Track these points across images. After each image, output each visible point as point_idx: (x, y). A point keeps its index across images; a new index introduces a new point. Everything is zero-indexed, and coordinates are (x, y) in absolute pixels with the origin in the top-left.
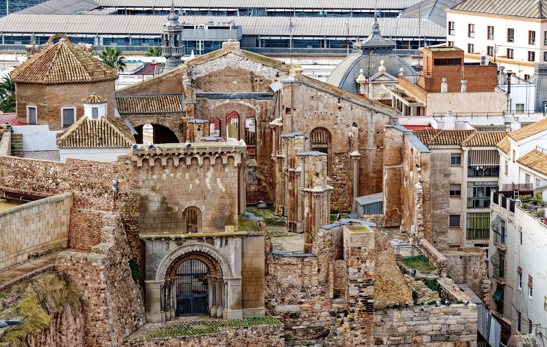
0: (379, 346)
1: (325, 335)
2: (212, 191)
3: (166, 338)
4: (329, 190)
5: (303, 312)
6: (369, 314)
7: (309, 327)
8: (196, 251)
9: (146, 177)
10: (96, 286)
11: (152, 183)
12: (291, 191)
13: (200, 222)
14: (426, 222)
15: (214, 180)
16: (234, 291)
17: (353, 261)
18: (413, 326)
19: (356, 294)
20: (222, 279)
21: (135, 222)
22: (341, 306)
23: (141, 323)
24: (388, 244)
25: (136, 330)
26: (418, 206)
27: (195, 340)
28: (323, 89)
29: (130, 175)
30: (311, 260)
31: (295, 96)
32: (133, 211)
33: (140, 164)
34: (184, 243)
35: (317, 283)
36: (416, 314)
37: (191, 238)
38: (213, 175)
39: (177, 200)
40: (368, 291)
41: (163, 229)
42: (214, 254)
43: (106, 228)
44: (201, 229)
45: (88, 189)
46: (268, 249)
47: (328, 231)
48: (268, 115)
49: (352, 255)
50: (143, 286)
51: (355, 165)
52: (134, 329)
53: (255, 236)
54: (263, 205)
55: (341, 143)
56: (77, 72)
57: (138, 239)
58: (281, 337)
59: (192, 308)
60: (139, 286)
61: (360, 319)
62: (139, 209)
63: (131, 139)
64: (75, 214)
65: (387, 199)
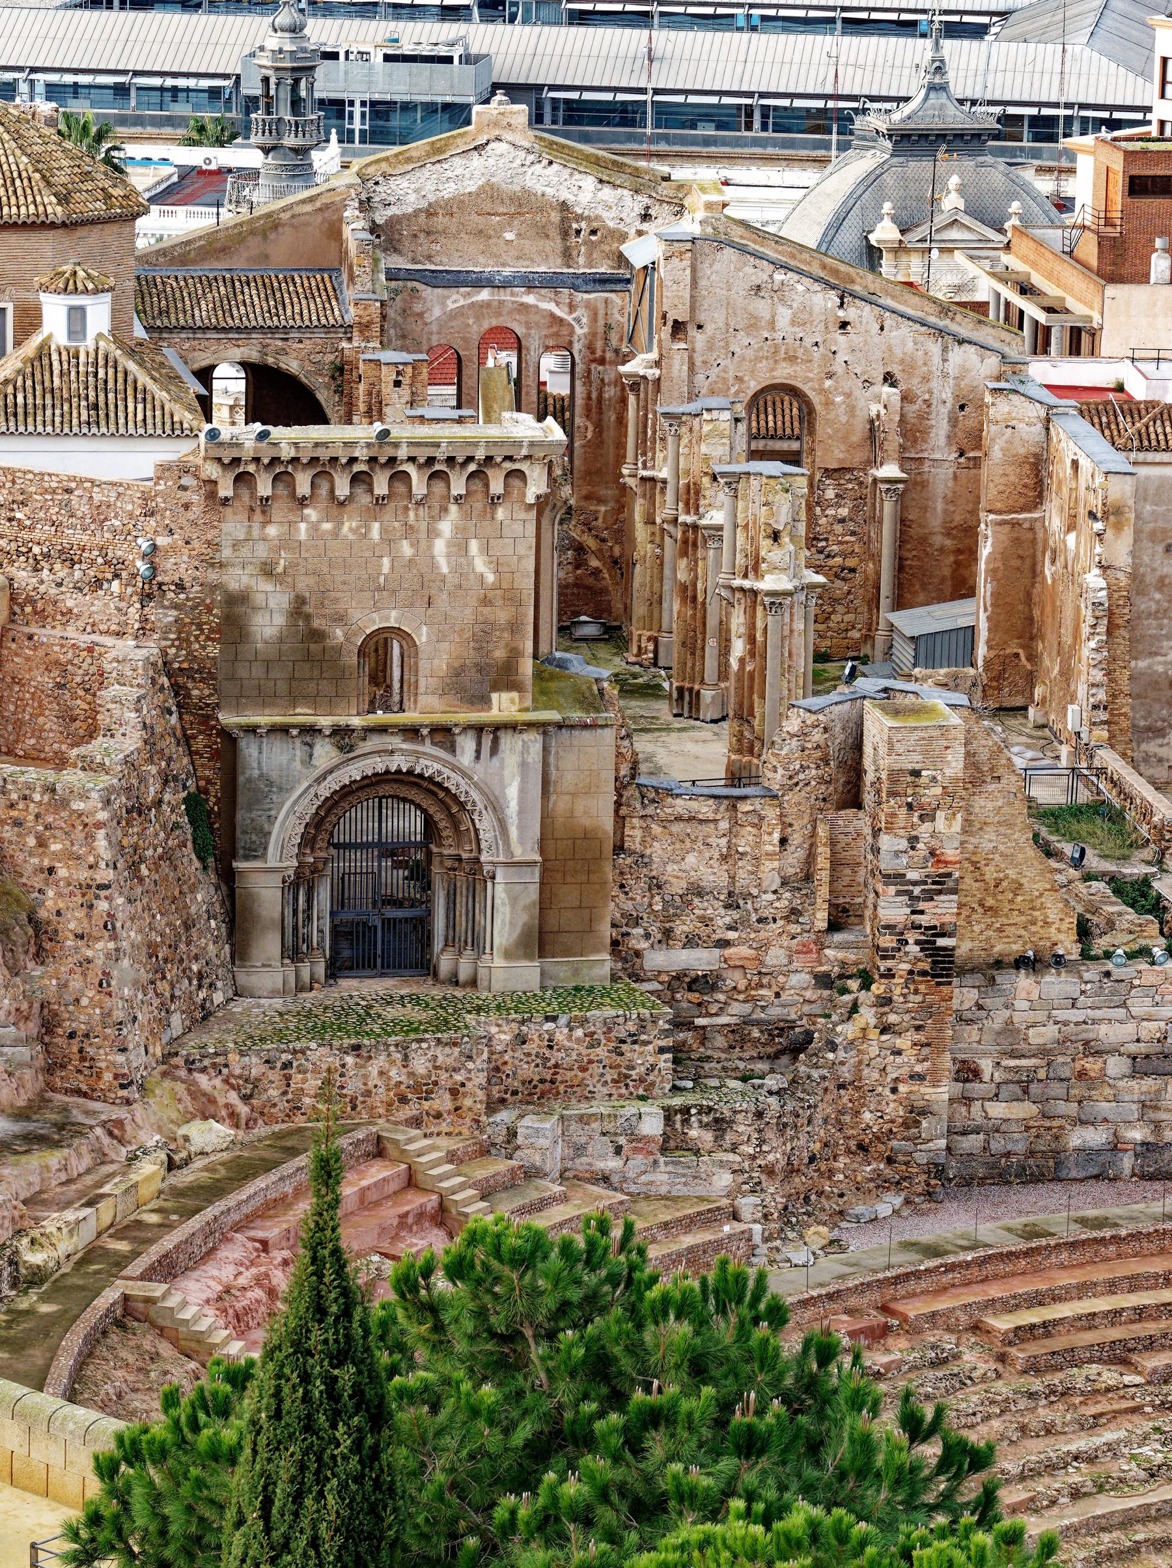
0: (968, 1085)
1: (797, 1048)
2: (452, 580)
3: (298, 1045)
4: (812, 587)
5: (730, 972)
6: (939, 984)
7: (747, 1022)
8: (399, 772)
9: (244, 530)
10: (83, 875)
11: (262, 551)
12: (684, 588)
13: (413, 679)
14: (1114, 696)
15: (459, 546)
16: (513, 901)
17: (893, 815)
18: (1077, 1024)
19: (902, 919)
20: (477, 861)
21: (204, 672)
22: (851, 956)
23: (218, 998)
24: (1004, 762)
25: (204, 1018)
26: (1092, 644)
27: (389, 1055)
28: (793, 263)
30: (758, 807)
31: (703, 283)
32: (202, 638)
33: (226, 490)
34: (361, 744)
35: (778, 881)
36: (1089, 986)
37: (382, 729)
38: (457, 529)
39: (341, 606)
40: (939, 911)
41: (293, 699)
42: (454, 782)
43: (115, 690)
44: (416, 702)
45: (57, 567)
46: (624, 770)
47: (814, 717)
48: (614, 342)
49: (892, 794)
50: (228, 878)
51: (888, 508)
52: (198, 1015)
53: (585, 726)
54: (591, 630)
55: (845, 439)
56: (20, 192)
57: (214, 727)
58: (662, 1050)
59: (379, 952)
60: (213, 878)
61: (911, 997)
62: (219, 631)
63: (189, 409)
64: (14, 646)
65: (989, 619)
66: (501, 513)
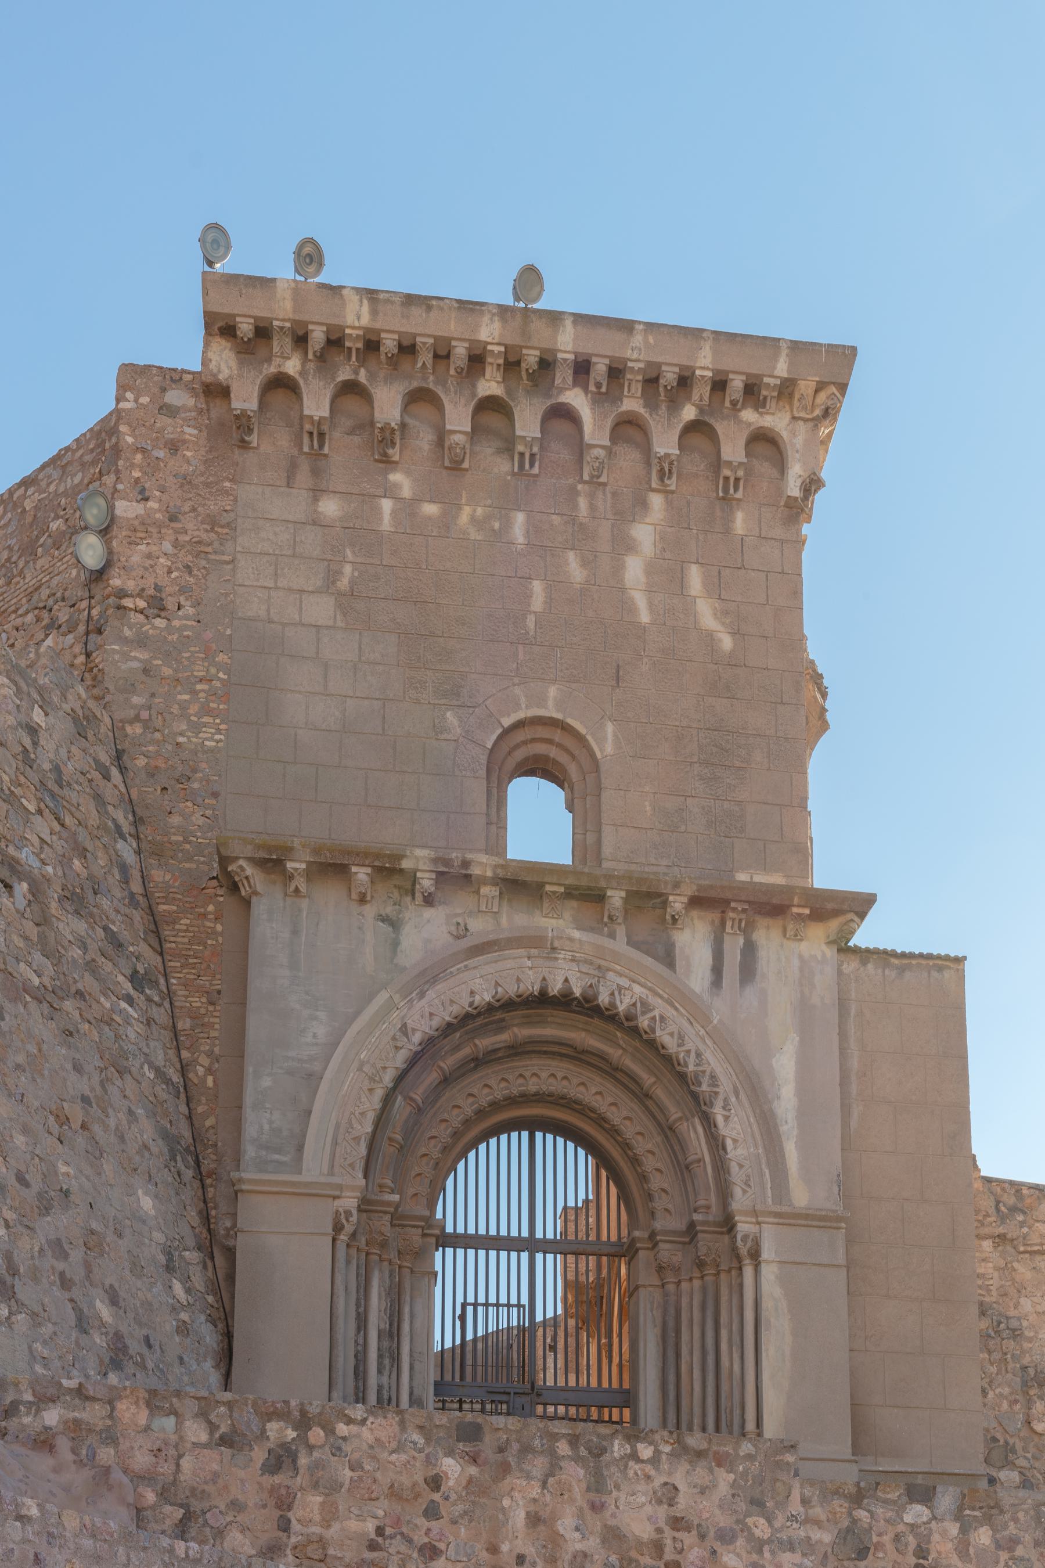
29: (186, 482)
66: (740, 522)
